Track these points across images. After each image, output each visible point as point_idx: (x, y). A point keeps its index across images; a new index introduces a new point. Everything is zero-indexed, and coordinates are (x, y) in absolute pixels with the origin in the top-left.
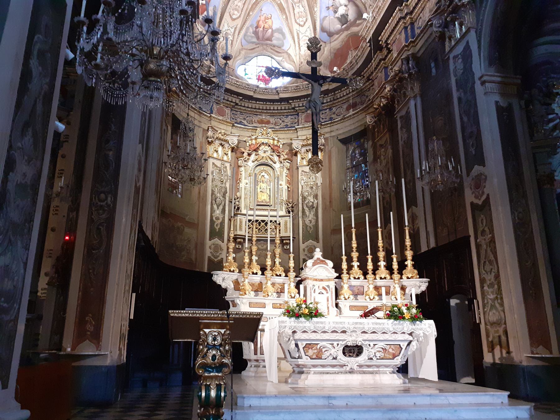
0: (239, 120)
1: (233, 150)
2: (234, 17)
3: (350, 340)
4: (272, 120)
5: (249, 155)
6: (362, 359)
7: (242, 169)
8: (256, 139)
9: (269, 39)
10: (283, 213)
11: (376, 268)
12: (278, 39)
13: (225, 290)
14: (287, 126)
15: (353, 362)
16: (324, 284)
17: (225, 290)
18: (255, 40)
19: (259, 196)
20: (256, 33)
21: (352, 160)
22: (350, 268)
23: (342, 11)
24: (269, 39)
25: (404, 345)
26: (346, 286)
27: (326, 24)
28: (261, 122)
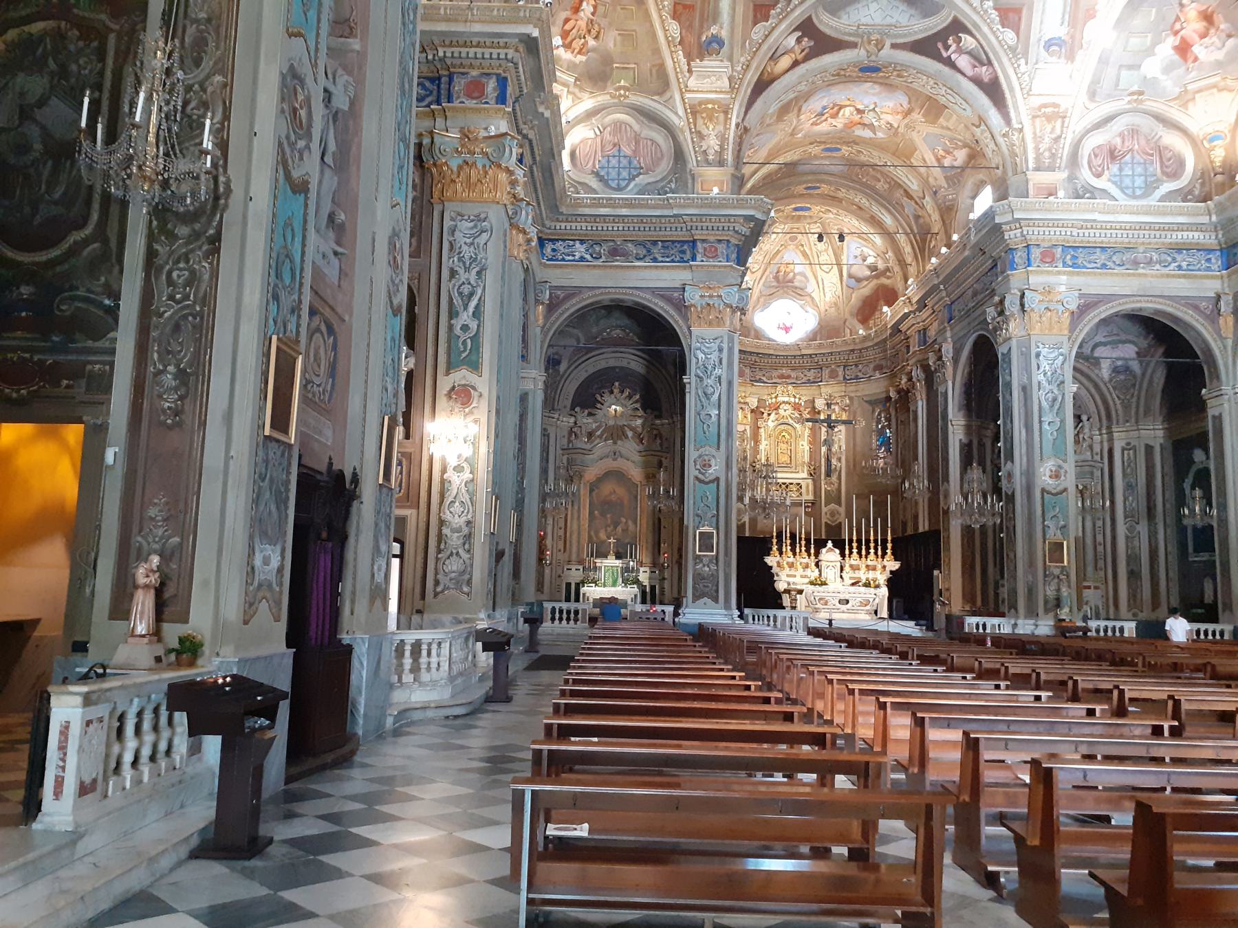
0: (758, 377)
1: (752, 411)
3: (842, 597)
4: (793, 374)
5: (769, 415)
6: (849, 606)
7: (762, 430)
8: (776, 397)
9: (791, 281)
10: (805, 475)
11: (868, 553)
12: (801, 281)
13: (771, 567)
14: (809, 381)
15: (844, 607)
16: (833, 564)
17: (771, 567)
18: (775, 284)
19: (780, 457)
20: (776, 278)
21: (879, 421)
22: (851, 553)
23: (870, 260)
24: (791, 281)
25: (871, 600)
26: (847, 565)
27: (854, 270)
28: (781, 377)
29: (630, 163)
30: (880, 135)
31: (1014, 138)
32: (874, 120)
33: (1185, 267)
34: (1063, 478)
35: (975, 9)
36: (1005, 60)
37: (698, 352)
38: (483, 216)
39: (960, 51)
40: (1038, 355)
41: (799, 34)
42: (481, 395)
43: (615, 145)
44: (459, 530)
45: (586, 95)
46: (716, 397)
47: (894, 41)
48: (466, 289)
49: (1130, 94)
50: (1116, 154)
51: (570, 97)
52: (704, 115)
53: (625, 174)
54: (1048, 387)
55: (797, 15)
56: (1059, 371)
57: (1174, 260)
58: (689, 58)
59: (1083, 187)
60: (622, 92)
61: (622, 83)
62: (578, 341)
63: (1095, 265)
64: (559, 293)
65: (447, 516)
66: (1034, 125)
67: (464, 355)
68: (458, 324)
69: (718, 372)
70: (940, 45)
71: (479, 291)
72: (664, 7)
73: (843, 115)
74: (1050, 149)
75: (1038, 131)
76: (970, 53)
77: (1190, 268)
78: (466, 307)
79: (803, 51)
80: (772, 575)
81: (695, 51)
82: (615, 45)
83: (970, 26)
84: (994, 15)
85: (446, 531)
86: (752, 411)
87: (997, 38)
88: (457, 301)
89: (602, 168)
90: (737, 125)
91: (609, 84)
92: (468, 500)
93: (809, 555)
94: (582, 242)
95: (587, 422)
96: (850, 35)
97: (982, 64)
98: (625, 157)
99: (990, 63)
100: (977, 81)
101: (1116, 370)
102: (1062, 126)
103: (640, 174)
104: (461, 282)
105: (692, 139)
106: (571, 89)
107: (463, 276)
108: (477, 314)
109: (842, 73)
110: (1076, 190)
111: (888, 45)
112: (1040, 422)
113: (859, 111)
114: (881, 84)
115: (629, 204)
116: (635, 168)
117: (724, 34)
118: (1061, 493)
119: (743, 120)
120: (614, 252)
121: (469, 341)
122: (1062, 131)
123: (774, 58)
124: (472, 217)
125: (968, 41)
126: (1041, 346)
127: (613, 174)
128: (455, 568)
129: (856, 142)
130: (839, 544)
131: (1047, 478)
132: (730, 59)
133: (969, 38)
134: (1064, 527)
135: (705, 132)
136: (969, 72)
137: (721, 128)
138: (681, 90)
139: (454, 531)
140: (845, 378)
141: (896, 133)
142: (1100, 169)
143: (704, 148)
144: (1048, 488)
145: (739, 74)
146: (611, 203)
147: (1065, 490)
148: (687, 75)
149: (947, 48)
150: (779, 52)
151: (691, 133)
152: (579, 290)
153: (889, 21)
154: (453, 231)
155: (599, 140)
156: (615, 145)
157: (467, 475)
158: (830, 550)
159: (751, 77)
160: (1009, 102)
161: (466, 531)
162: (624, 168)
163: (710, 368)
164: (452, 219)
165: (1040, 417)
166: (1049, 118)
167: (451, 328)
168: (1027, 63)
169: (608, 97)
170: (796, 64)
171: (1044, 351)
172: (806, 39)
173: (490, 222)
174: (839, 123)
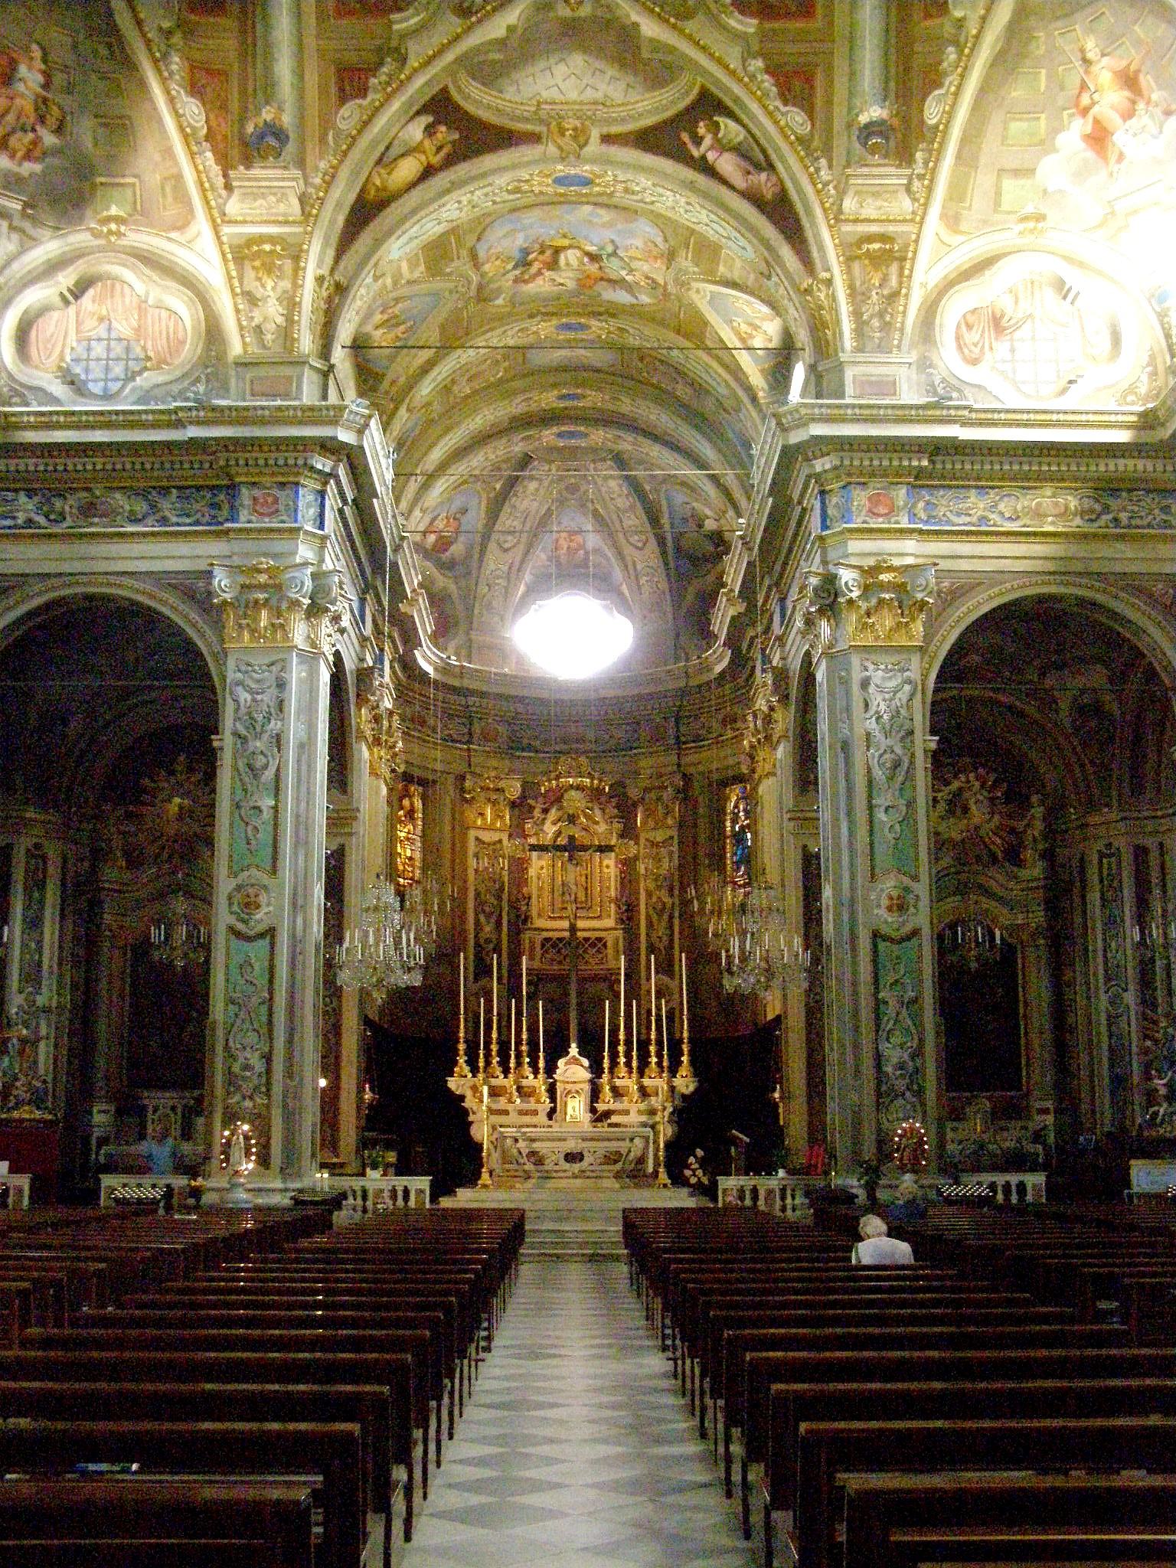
1: (513, 805)
2: (506, 546)
5: (545, 811)
6: (584, 1164)
8: (557, 778)
10: (609, 922)
13: (462, 1098)
15: (576, 1167)
17: (462, 1098)
29: (128, 349)
30: (645, 299)
31: (822, 296)
32: (623, 273)
33: (1125, 522)
34: (912, 910)
35: (732, 73)
36: (792, 160)
37: (240, 689)
39: (721, 147)
40: (865, 684)
41: (430, 119)
45: (47, 233)
46: (269, 774)
47: (605, 130)
49: (1024, 219)
50: (1004, 323)
51: (15, 236)
52: (257, 263)
53: (118, 370)
54: (884, 743)
55: (419, 86)
56: (903, 712)
57: (1106, 509)
58: (225, 163)
59: (943, 381)
61: (114, 211)
63: (967, 519)
66: (849, 271)
69: (274, 726)
70: (685, 137)
72: (171, 73)
73: (568, 264)
74: (881, 315)
75: (858, 283)
76: (738, 150)
77: (1133, 522)
79: (439, 149)
80: (466, 1112)
81: (235, 153)
82: (96, 145)
83: (729, 103)
84: (767, 82)
86: (513, 805)
87: (776, 123)
89: (76, 360)
90: (320, 280)
91: (89, 213)
93: (536, 1072)
94: (30, 493)
96: (527, 120)
97: (759, 168)
98: (120, 340)
99: (771, 167)
100: (753, 197)
101: (1081, 711)
102: (901, 275)
103: (146, 369)
105: (235, 305)
106: (16, 223)
109: (526, 187)
110: (933, 385)
111: (595, 134)
112: (871, 807)
113: (594, 258)
114: (607, 206)
115: (105, 421)
117: (287, 120)
118: (908, 938)
119: (332, 270)
122: (901, 283)
123: (385, 161)
125: (730, 129)
126: (871, 667)
127: (97, 372)
129: (612, 312)
130: (592, 1049)
131: (882, 912)
132: (301, 163)
133: (731, 124)
134: (914, 1001)
135: (259, 293)
136: (739, 182)
137: (286, 284)
138: (214, 221)
140: (678, 742)
141: (666, 295)
142: (977, 350)
143: (256, 322)
144: (885, 930)
145: (318, 189)
146: (75, 421)
147: (915, 933)
148: (224, 193)
149: (698, 141)
150: (394, 151)
151: (234, 295)
152: (24, 578)
153: (590, 95)
156: (101, 319)
158: (575, 1061)
159: (342, 196)
160: (809, 234)
163: (260, 718)
165: (870, 797)
166: (879, 260)
168: (830, 167)
170: (428, 172)
171: (877, 676)
172: (443, 128)
174: (566, 278)
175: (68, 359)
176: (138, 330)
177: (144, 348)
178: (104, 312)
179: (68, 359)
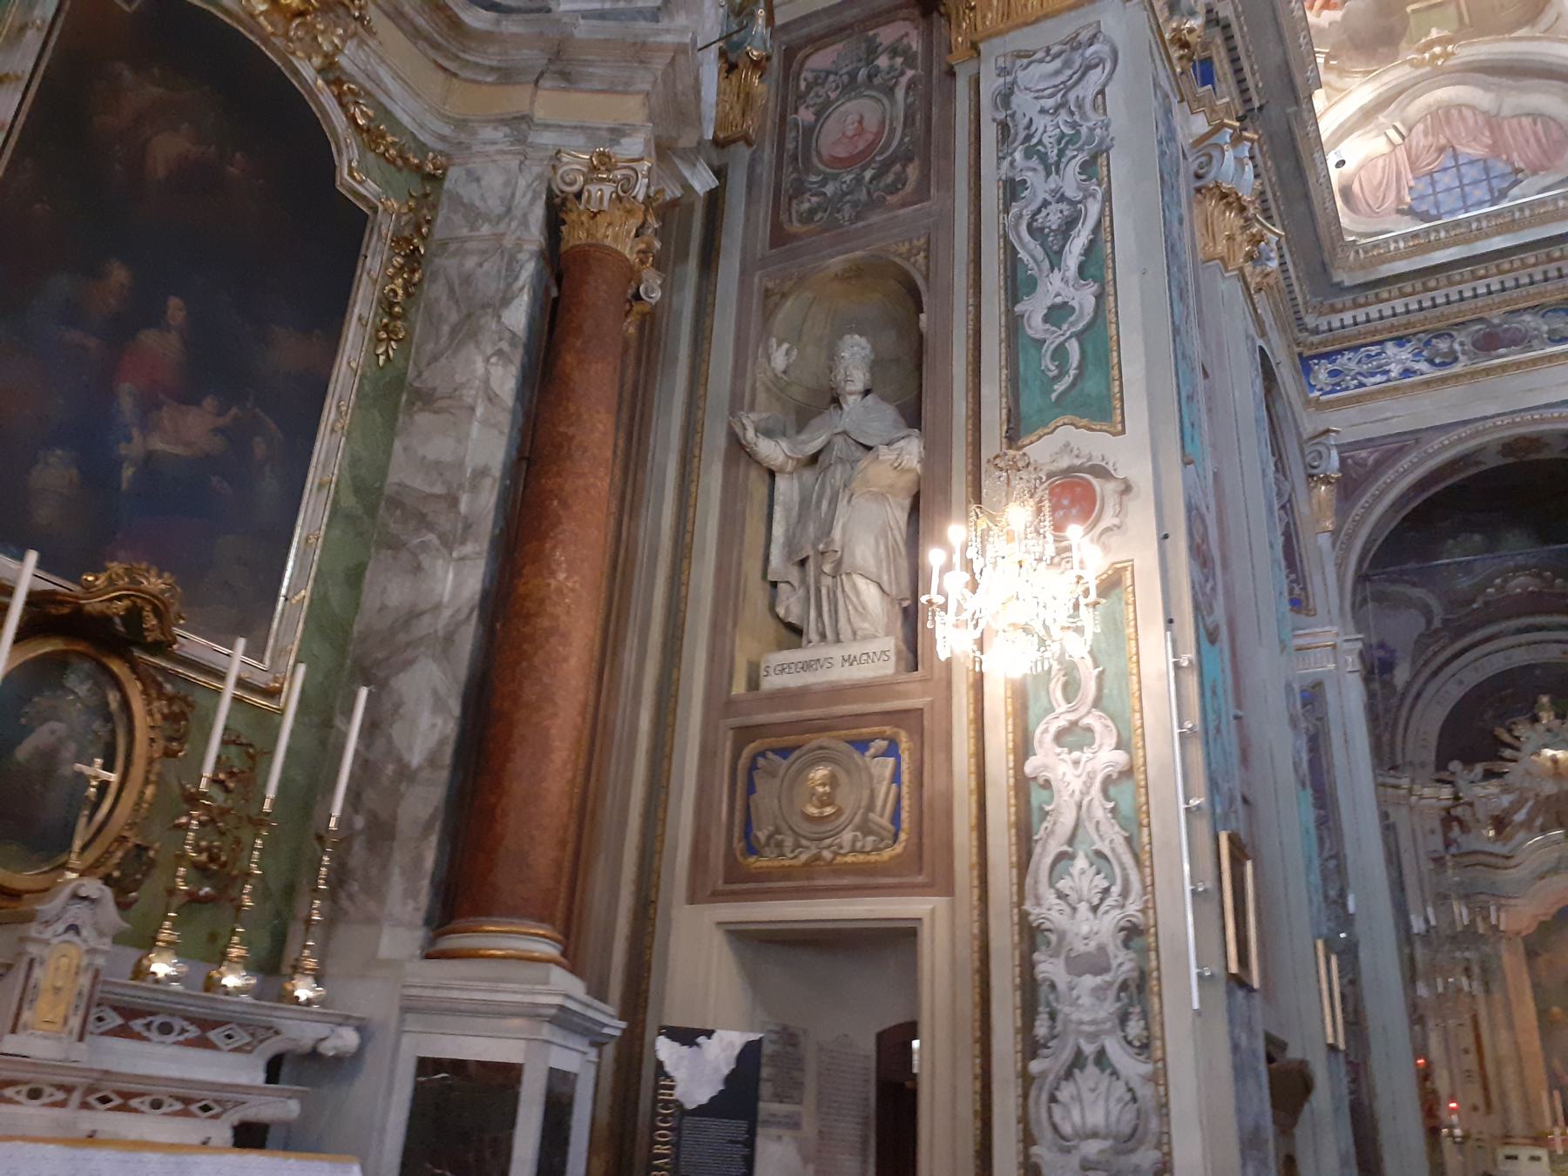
38: (1084, 36)
42: (1127, 489)
43: (1441, 150)
44: (1096, 963)
45: (1353, 82)
48: (1053, 217)
60: (1437, 50)
61: (1434, 33)
62: (1428, 614)
64: (1364, 454)
65: (1048, 910)
67: (1060, 387)
68: (1034, 309)
71: (1094, 208)
78: (1055, 258)
85: (1049, 968)
88: (1030, 251)
89: (1421, 198)
91: (1403, 45)
92: (1122, 849)
94: (1400, 341)
95: (1487, 795)
98: (1472, 162)
104: (1034, 206)
107: (1039, 185)
108: (1094, 265)
116: (1503, 176)
120: (1489, 342)
121: (1074, 347)
124: (1055, 50)
128: (1096, 1118)
139: (1082, 964)
152: (1416, 437)
154: (1005, 97)
155: (1401, 154)
157: (1105, 757)
161: (1123, 963)
162: (1475, 183)
164: (1003, 72)
167: (1014, 325)
169: (1407, 69)
173: (1107, 40)
175: (1408, 199)
176: (1494, 147)
177: (1509, 162)
178: (1443, 141)
179: (1408, 199)
